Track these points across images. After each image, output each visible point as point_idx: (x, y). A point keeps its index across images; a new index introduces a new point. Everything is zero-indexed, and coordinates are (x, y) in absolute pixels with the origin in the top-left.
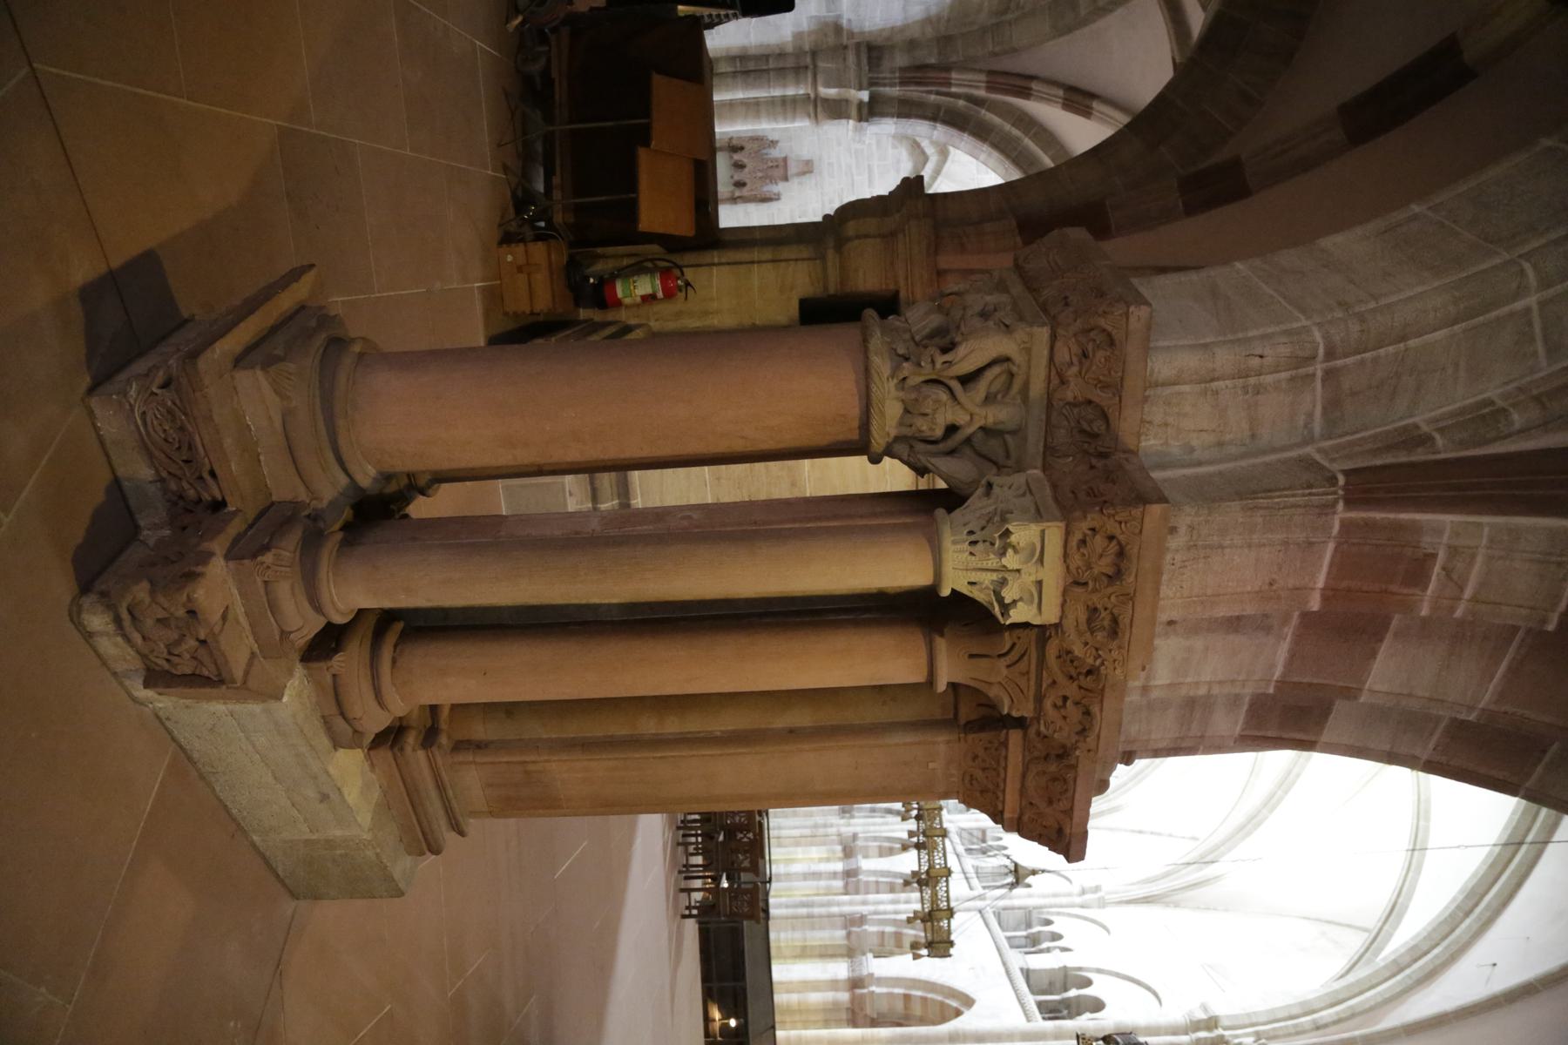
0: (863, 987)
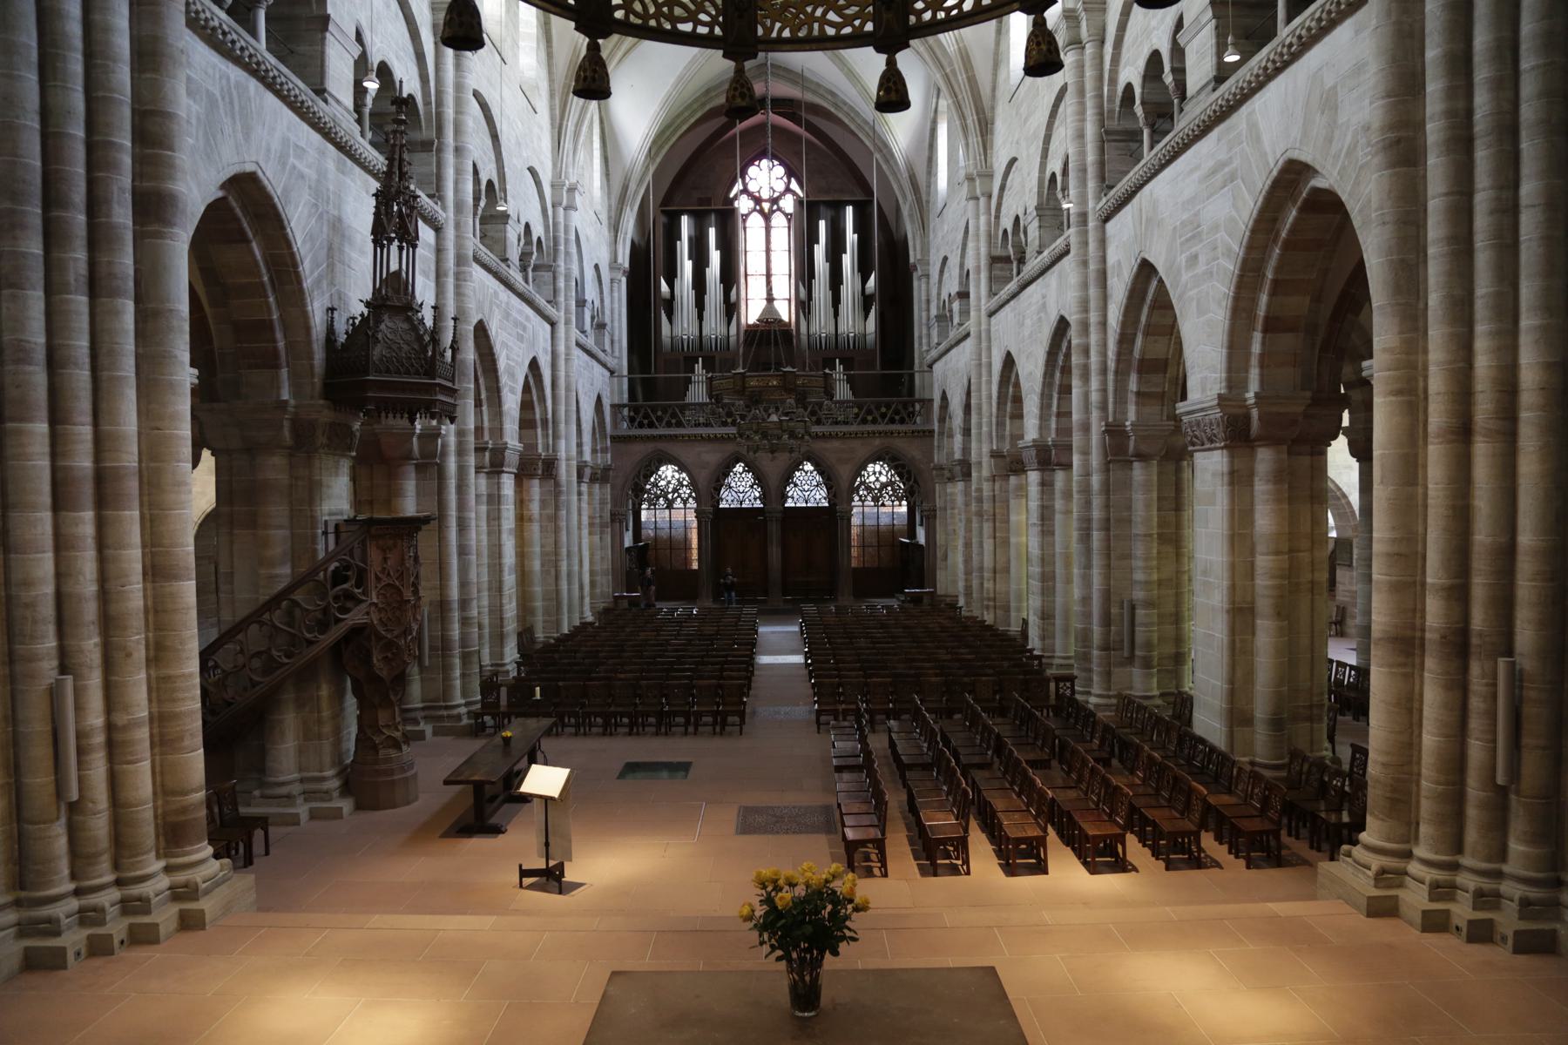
0: (1248, 417)
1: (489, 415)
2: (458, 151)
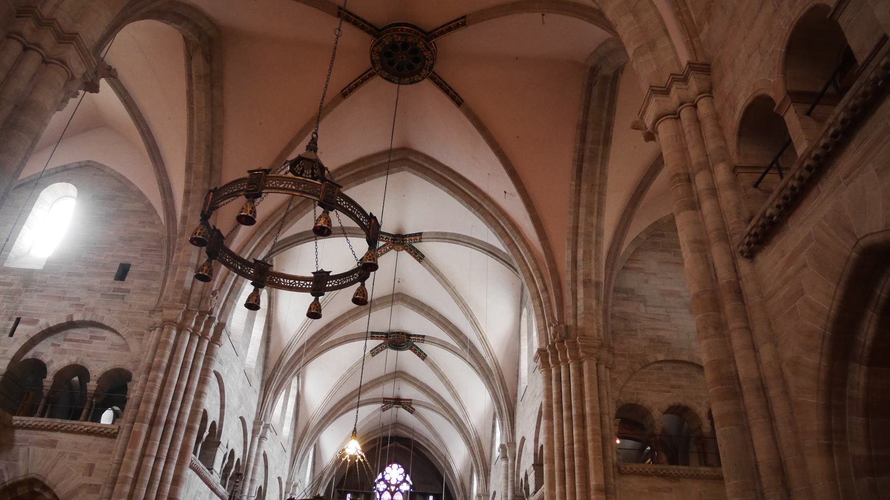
2: (252, 481)
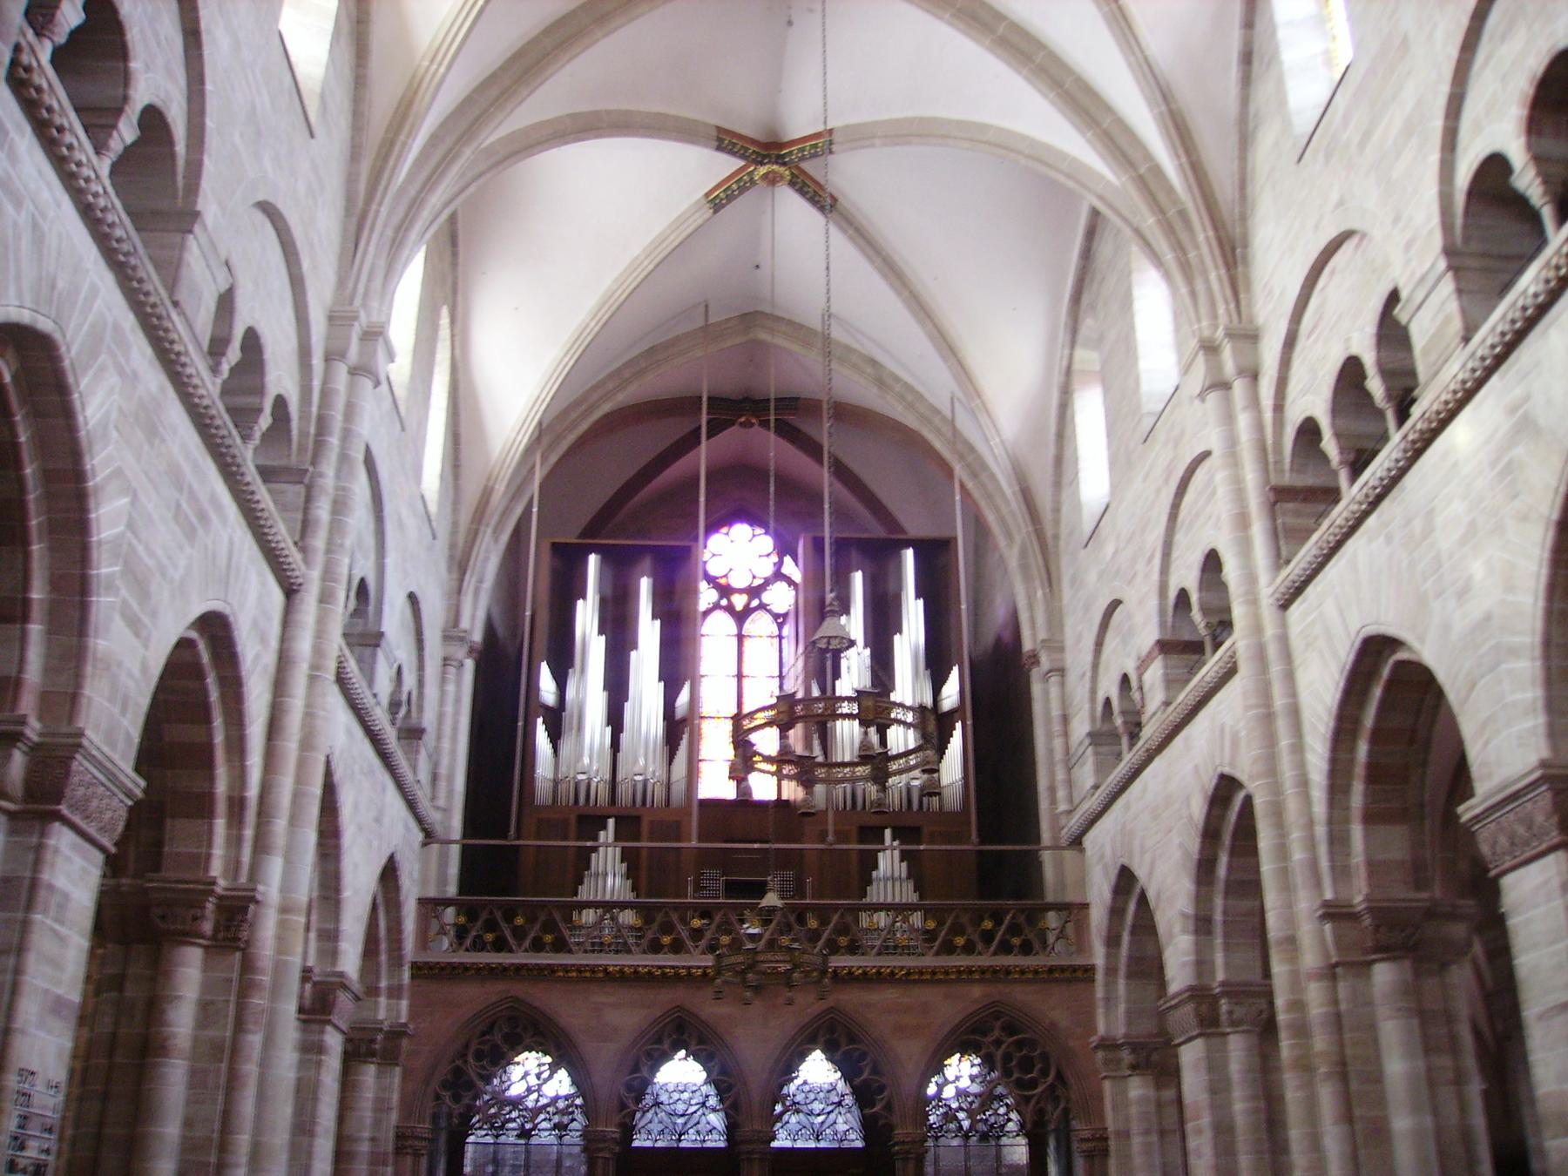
1: (48, 656)
